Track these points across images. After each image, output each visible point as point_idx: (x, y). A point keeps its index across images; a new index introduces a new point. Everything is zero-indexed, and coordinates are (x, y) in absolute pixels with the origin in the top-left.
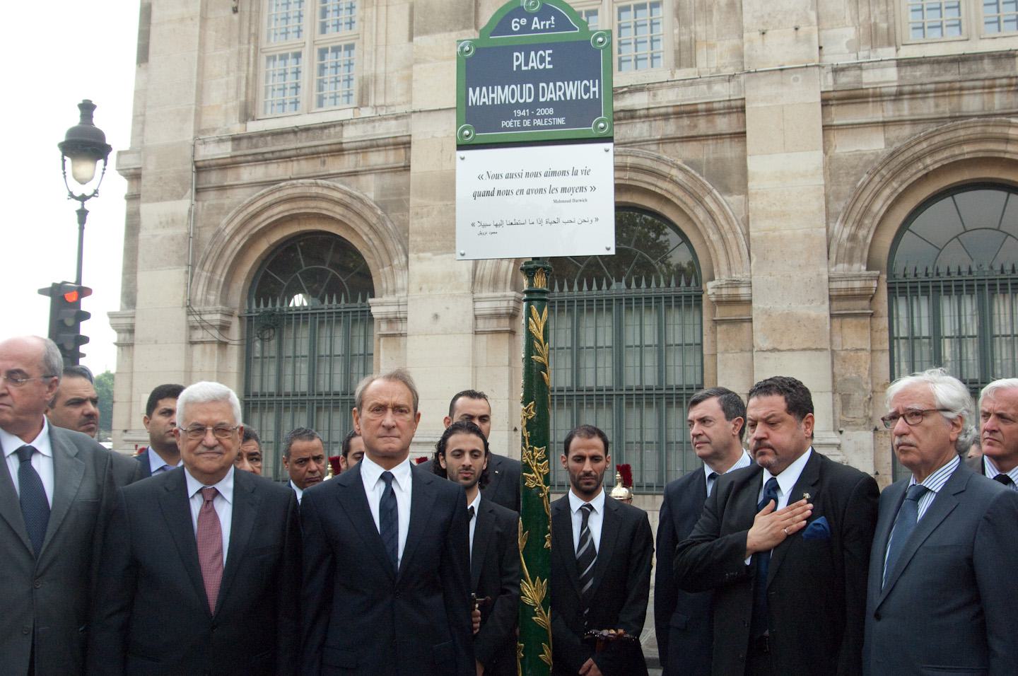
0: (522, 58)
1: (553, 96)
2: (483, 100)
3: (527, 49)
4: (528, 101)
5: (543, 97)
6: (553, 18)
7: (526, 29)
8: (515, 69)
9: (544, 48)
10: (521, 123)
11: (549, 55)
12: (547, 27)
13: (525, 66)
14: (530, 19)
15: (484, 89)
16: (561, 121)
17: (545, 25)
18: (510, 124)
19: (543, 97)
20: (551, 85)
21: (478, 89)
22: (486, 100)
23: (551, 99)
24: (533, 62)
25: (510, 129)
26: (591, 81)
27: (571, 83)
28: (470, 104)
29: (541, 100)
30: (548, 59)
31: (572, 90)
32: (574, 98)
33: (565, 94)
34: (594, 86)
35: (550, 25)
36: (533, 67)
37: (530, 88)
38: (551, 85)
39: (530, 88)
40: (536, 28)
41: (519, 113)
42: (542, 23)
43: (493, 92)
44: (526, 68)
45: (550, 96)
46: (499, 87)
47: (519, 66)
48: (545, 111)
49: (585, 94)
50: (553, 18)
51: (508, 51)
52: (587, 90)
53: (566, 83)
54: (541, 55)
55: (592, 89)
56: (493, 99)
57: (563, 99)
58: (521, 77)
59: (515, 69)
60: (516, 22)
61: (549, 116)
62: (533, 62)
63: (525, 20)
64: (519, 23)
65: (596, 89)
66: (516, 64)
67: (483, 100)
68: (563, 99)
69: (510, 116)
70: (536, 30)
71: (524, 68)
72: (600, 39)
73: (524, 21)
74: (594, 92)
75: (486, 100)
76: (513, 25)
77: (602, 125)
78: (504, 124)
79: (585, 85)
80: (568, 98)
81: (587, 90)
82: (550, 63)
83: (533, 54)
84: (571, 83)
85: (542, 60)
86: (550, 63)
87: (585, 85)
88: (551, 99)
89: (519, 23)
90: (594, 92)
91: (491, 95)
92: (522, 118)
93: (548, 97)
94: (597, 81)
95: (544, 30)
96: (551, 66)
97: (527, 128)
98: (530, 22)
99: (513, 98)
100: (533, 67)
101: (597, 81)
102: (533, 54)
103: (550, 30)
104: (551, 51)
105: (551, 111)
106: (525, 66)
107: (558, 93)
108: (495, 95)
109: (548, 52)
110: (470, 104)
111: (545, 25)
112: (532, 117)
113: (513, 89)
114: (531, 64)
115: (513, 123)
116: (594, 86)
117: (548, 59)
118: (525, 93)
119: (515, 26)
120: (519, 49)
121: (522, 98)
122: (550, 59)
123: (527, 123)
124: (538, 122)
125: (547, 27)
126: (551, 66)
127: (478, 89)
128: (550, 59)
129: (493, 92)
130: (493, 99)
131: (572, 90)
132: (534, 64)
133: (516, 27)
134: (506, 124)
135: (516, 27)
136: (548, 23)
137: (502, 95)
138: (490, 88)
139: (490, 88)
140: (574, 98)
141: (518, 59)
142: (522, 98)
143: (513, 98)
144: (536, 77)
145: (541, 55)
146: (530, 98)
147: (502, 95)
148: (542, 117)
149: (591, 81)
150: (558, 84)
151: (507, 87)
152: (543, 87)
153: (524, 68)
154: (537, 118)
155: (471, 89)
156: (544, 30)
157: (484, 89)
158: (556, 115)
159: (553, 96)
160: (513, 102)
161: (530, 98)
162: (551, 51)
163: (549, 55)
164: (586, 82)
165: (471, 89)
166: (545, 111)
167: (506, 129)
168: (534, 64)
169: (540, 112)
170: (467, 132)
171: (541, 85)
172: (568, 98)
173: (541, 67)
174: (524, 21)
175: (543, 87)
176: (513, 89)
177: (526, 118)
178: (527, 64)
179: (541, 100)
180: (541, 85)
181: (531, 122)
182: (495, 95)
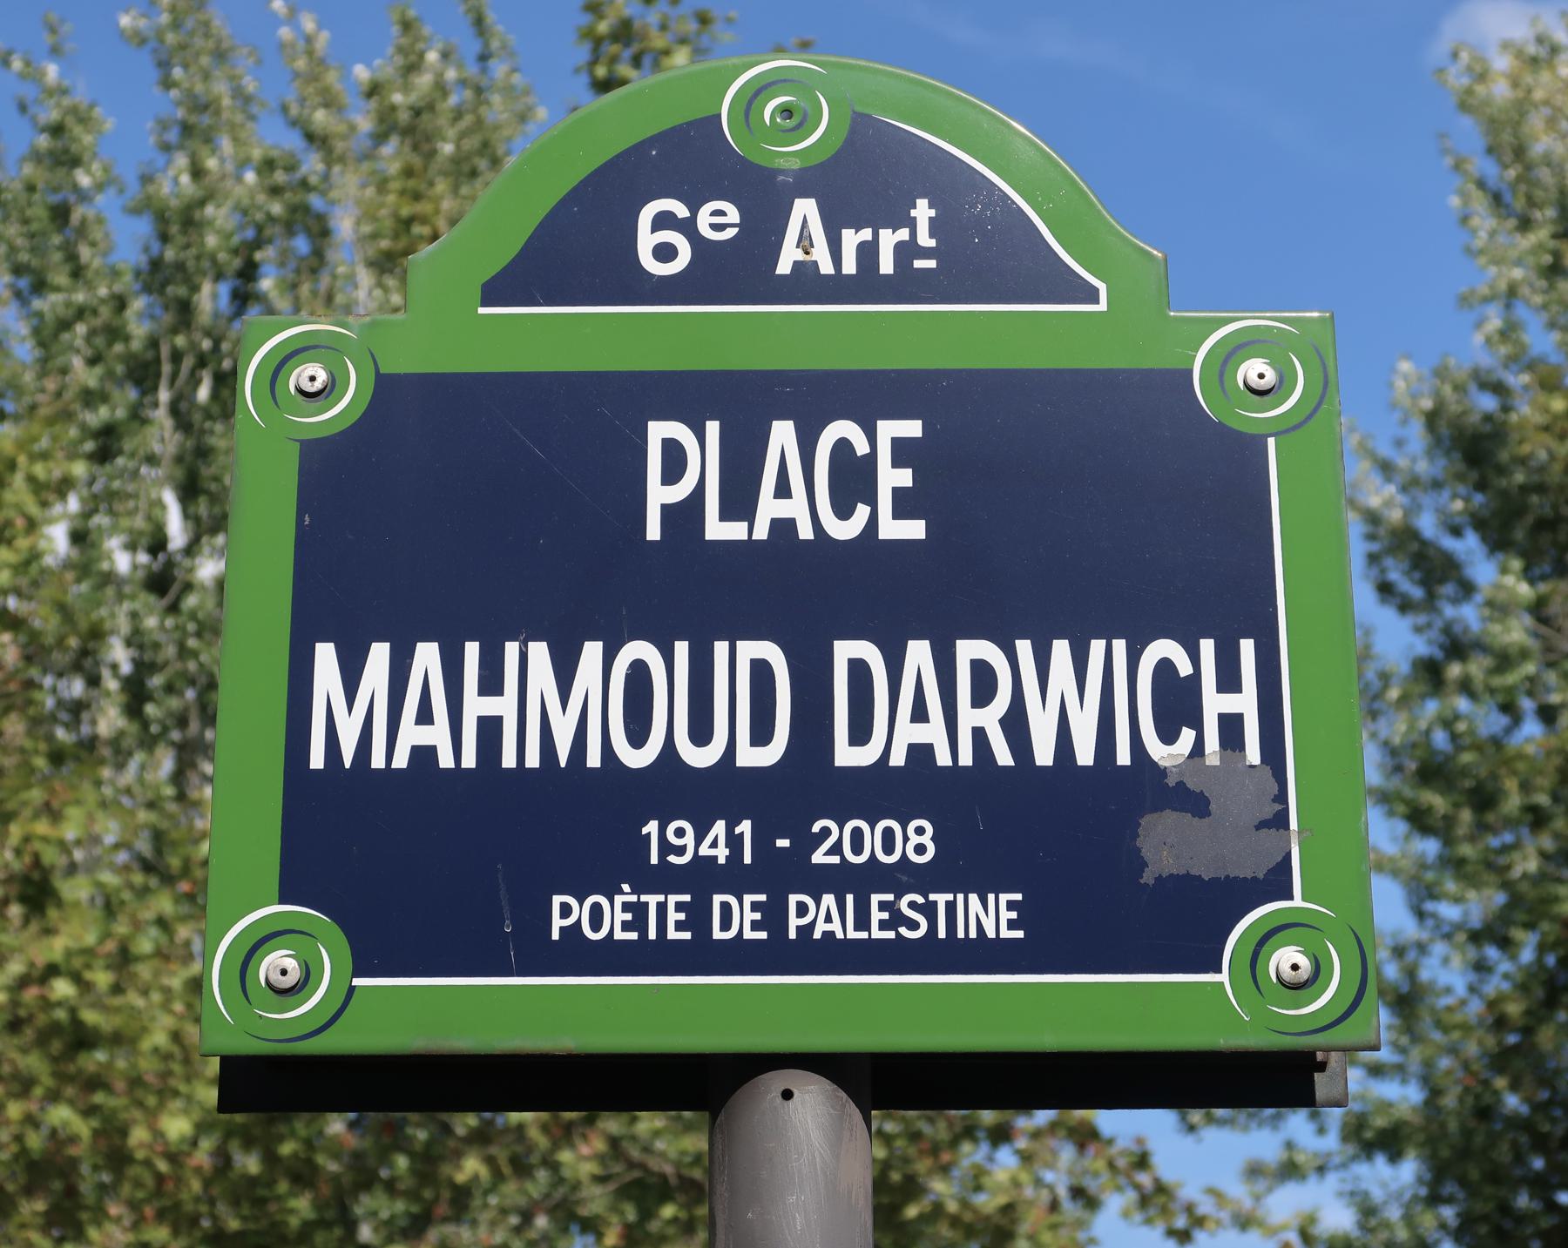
0: (705, 454)
1: (933, 732)
2: (411, 735)
3: (741, 405)
4: (750, 757)
5: (860, 734)
6: (923, 211)
7: (733, 271)
8: (654, 532)
9: (869, 396)
10: (697, 917)
11: (903, 452)
12: (886, 266)
13: (725, 515)
14: (765, 206)
15: (427, 656)
16: (990, 915)
17: (868, 252)
18: (616, 918)
19: (860, 734)
20: (919, 654)
21: (380, 654)
22: (437, 735)
23: (921, 753)
24: (783, 490)
25: (610, 957)
26: (1207, 647)
27: (1061, 650)
28: (317, 761)
29: (847, 755)
30: (892, 478)
31: (1067, 700)
32: (1085, 755)
33: (1016, 723)
34: (1229, 681)
35: (905, 252)
36: (782, 527)
37: (761, 671)
38: (919, 654)
39: (761, 671)
40: (804, 270)
41: (681, 840)
42: (851, 239)
43: (491, 684)
44: (735, 531)
45: (908, 733)
46: (539, 652)
47: (686, 516)
48: (873, 841)
49: (1168, 735)
50: (923, 211)
51: (608, 410)
52: (1177, 703)
53: (1024, 648)
54: (843, 446)
55: (1214, 703)
56: (490, 729)
57: (1004, 756)
58: (696, 592)
59: (654, 532)
60: (663, 221)
61: (902, 877)
62: (783, 490)
63: (733, 214)
64: (688, 227)
65: (1246, 703)
66: (659, 495)
67: (411, 735)
68: (1004, 756)
69: (622, 864)
70: (806, 285)
71: (717, 529)
72: (1255, 370)
73: (720, 219)
74: (1231, 726)
75: (437, 735)
76: (646, 241)
77: (1287, 958)
78: (567, 913)
79: (1165, 668)
80: (1044, 755)
81: (1177, 703)
82: (904, 505)
83: (783, 434)
84: (1061, 650)
85: (853, 479)
86: (904, 505)
87: (1165, 668)
88: (921, 753)
89: (688, 227)
90: (1231, 726)
91: (476, 706)
92: (702, 879)
93: (898, 737)
94: (1247, 647)
95: (866, 284)
96: (915, 529)
97: (738, 957)
98: (764, 227)
99: (638, 738)
100: (782, 527)
101: (1247, 647)
102: (783, 434)
103: (905, 285)
104: (912, 428)
105: (918, 841)
106: (725, 515)
107: (968, 717)
108: (503, 706)
109: (889, 430)
110: (317, 761)
111: (868, 252)
112: (780, 875)
113: (639, 675)
114: (769, 508)
115: (639, 910)
116: (1229, 681)
117: (892, 478)
118: (721, 705)
119: (655, 240)
120: (689, 395)
121: (701, 733)
122: (905, 478)
123: (740, 916)
124: (824, 916)
125: (886, 266)
126: (915, 529)
127: (380, 654)
128: (905, 478)
129: (491, 684)
130: (490, 729)
131: (1067, 700)
132: (795, 508)
133: (665, 253)
134: (581, 913)
135: (665, 253)
136: (889, 240)
137: (556, 703)
138: (472, 650)
139: (472, 650)
140: (1085, 755)
141: (677, 467)
142: (701, 733)
143: (638, 738)
144: (805, 594)
145: (843, 446)
146: (762, 734)
147: (556, 703)
148: (841, 880)
149: (1207, 647)
150: (968, 650)
151: (592, 652)
152: (859, 670)
153: (717, 529)
154: (819, 882)
155: (326, 656)
156: (866, 284)
157: (427, 656)
158: (956, 870)
159: (933, 732)
160: (637, 759)
161: (762, 734)
162: (912, 428)
163: (903, 452)
164: (1164, 648)
165: (326, 656)
166: (873, 841)
167: (578, 954)
168: (793, 502)
169: (838, 840)
170: (278, 963)
171: (845, 651)
172: (1044, 755)
173: (844, 530)
174: (720, 219)
175: (859, 670)
176: (639, 671)
177: (734, 878)
178: (739, 504)
179: (847, 755)
180: (845, 651)
181: (773, 916)
182: (503, 706)
